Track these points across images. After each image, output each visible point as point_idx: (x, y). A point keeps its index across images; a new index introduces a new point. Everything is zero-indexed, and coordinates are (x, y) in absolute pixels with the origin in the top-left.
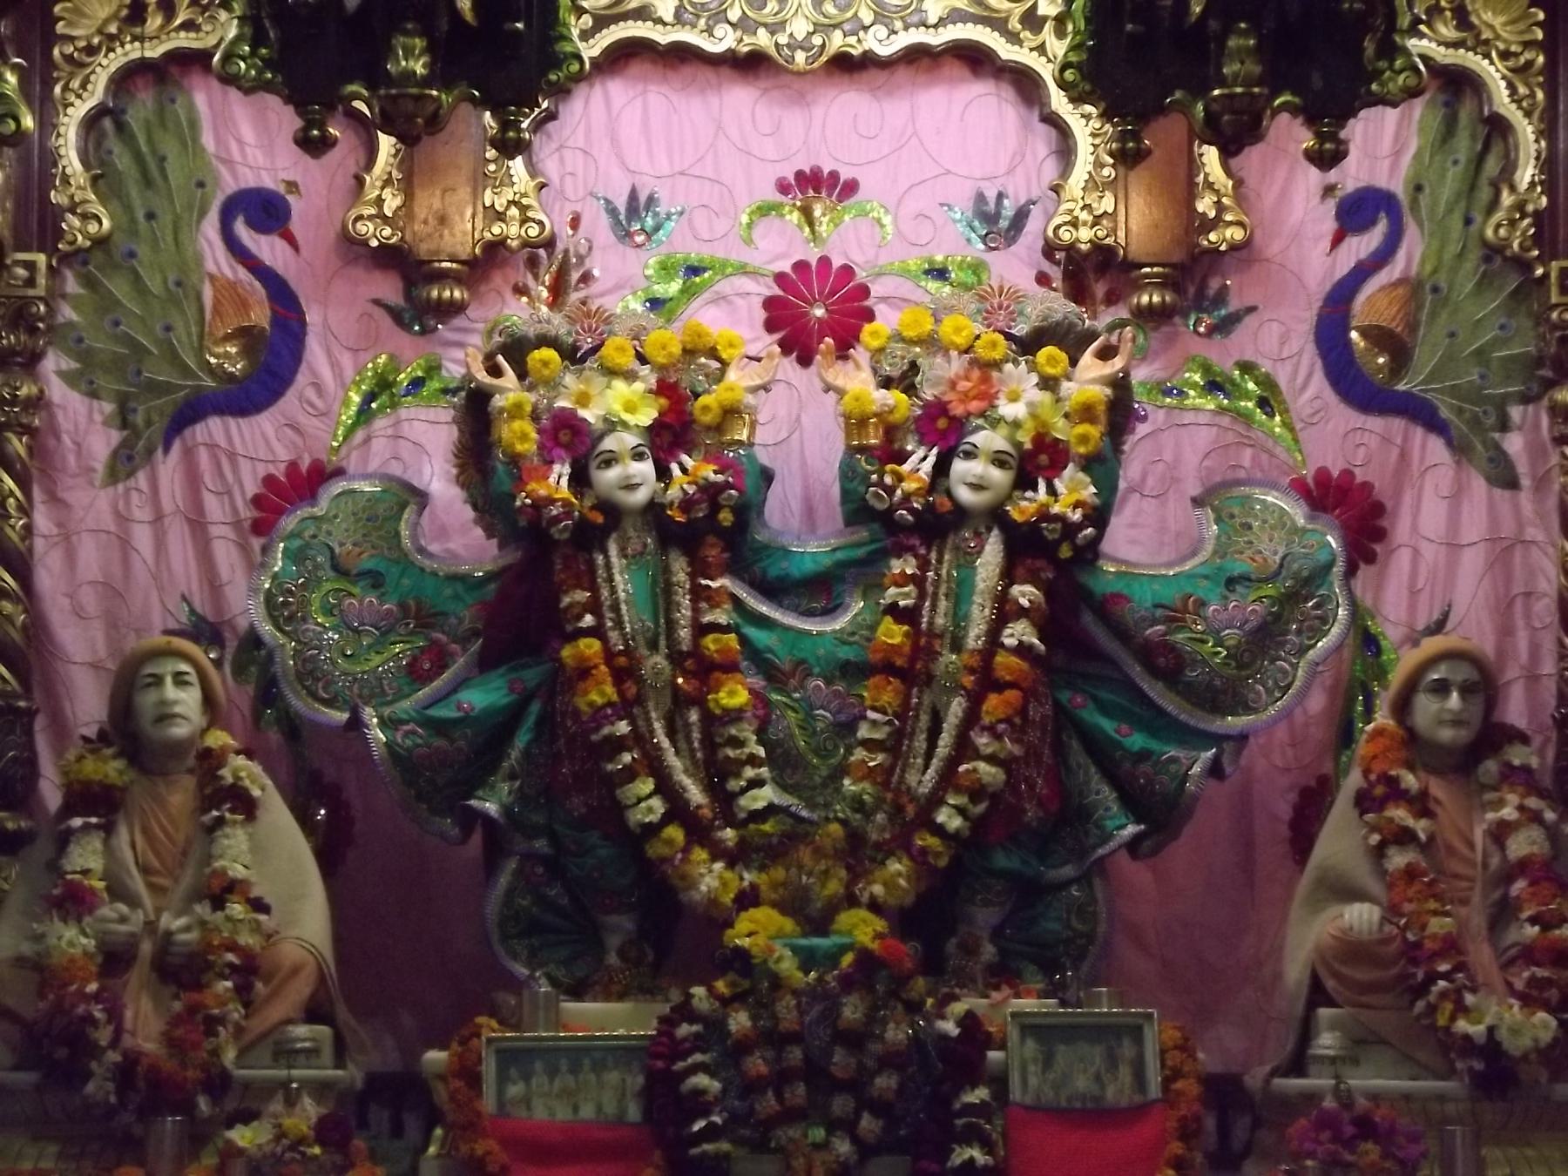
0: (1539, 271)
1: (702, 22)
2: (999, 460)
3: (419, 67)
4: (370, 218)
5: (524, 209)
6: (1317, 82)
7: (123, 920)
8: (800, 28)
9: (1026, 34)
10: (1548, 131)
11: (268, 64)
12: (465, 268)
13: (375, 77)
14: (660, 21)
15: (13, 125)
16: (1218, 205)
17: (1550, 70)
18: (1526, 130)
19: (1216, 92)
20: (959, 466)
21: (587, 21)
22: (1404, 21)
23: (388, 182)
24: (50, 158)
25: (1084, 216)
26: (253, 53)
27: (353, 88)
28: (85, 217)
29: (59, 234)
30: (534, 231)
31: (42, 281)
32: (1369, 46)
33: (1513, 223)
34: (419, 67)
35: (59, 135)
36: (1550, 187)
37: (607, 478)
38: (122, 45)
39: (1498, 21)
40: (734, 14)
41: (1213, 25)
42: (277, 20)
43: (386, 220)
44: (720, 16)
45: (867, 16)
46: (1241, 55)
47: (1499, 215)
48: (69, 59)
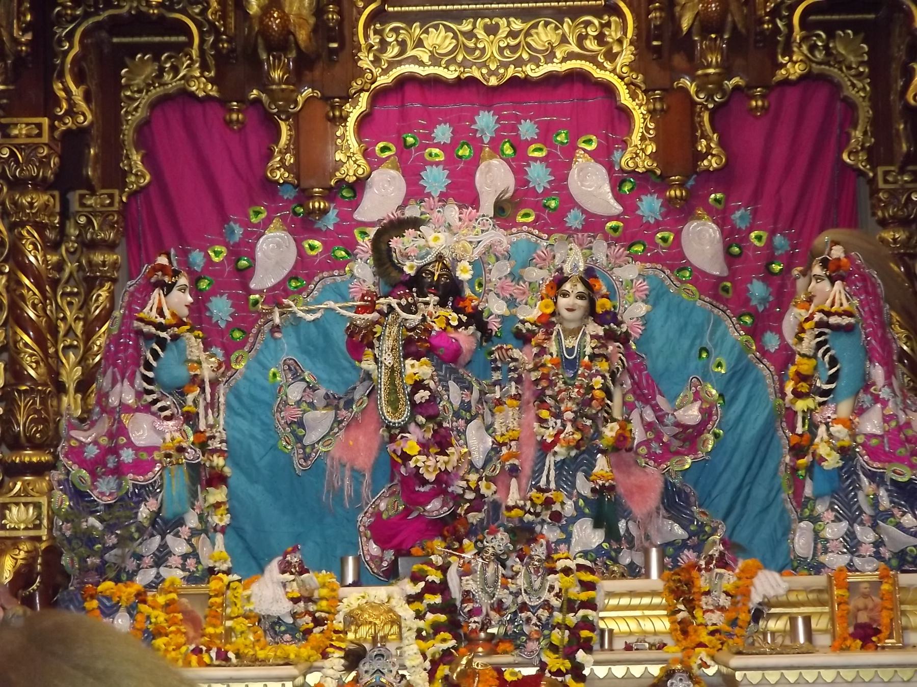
0: (871, 174)
1: (443, 62)
4: (278, 168)
9: (608, 65)
12: (327, 192)
14: (421, 63)
15: (82, 118)
16: (709, 147)
19: (700, 72)
26: (202, 75)
31: (117, 204)
32: (779, 50)
35: (124, 135)
38: (155, 88)
40: (460, 58)
43: (287, 169)
45: (525, 56)
48: (128, 97)
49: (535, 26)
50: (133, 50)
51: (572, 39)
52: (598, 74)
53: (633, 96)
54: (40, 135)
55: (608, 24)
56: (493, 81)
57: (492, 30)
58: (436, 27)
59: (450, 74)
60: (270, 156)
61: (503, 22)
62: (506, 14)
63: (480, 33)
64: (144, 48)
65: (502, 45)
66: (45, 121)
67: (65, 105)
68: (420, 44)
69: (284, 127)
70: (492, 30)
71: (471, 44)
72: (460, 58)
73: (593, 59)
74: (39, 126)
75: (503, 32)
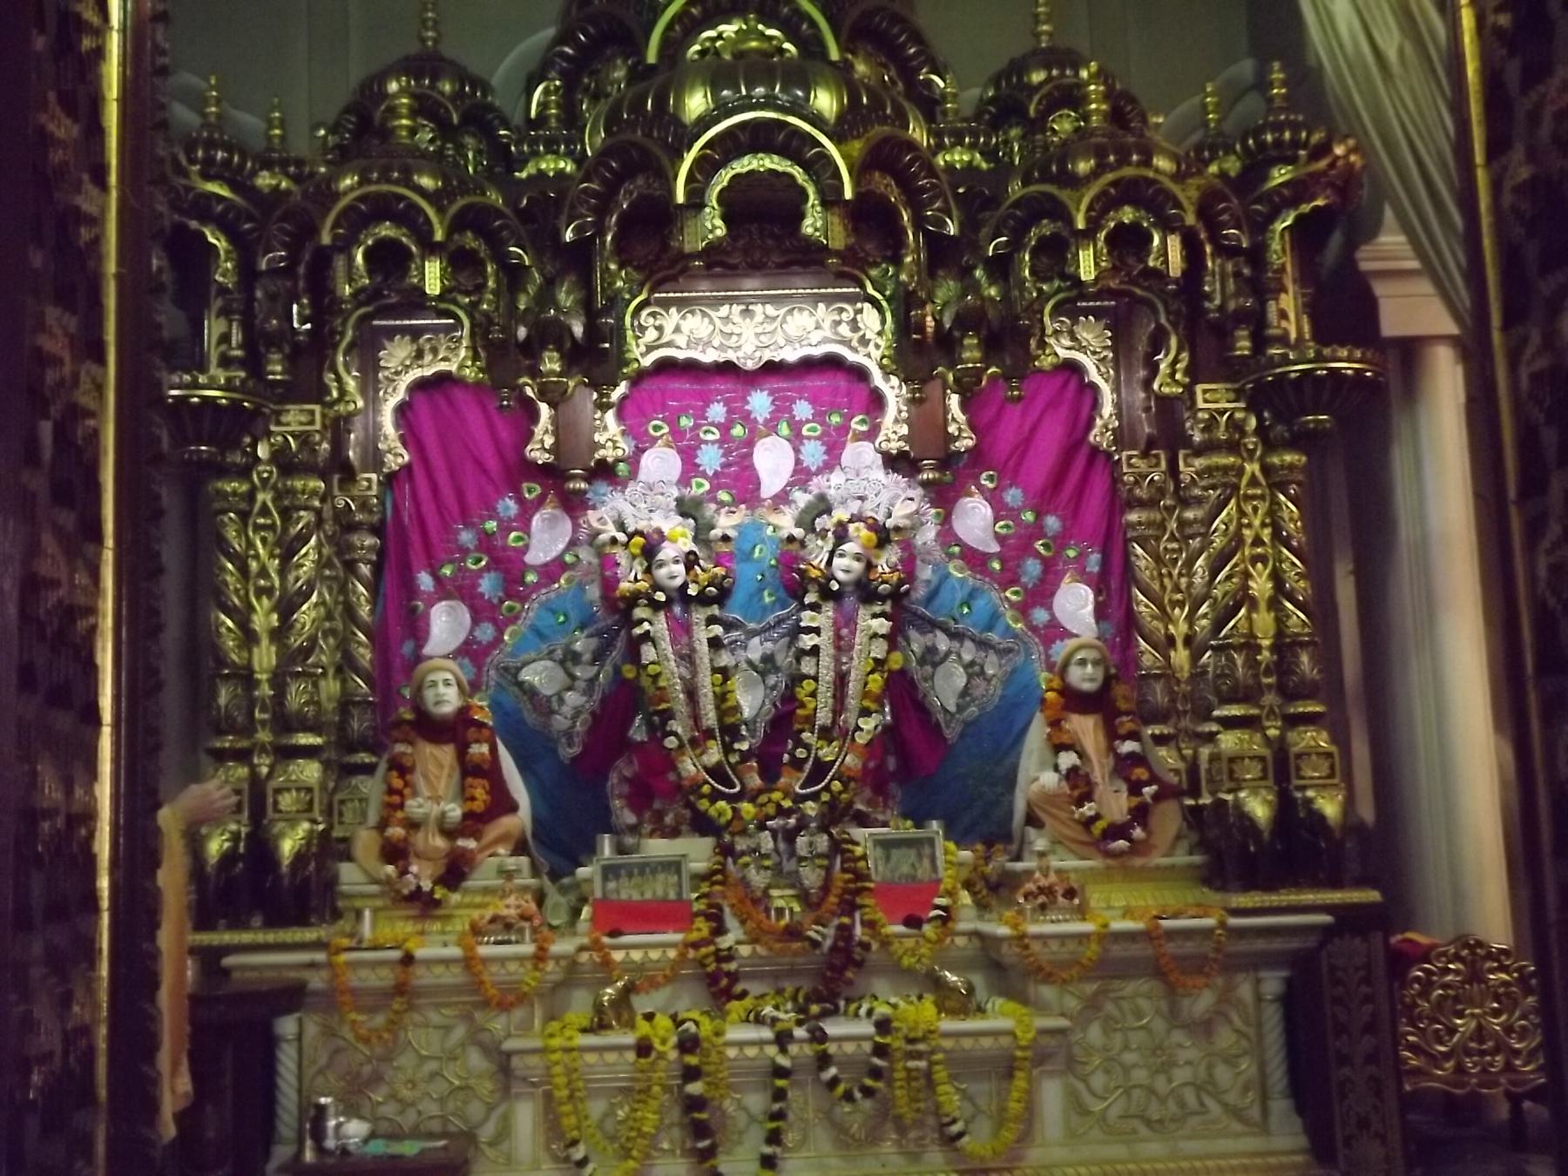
2: (857, 557)
3: (557, 367)
5: (614, 442)
6: (1008, 362)
7: (420, 806)
8: (748, 348)
10: (1116, 389)
11: (481, 370)
13: (535, 373)
16: (960, 429)
17: (1116, 360)
18: (1106, 388)
20: (837, 561)
21: (643, 349)
22: (1049, 331)
23: (546, 431)
24: (378, 427)
25: (893, 436)
27: (522, 380)
28: (396, 455)
29: (383, 463)
30: (620, 453)
32: (1033, 343)
33: (1102, 434)
34: (557, 367)
36: (1119, 416)
37: (661, 573)
39: (1089, 337)
40: (716, 343)
41: (957, 334)
42: (484, 347)
44: (708, 343)
45: (782, 342)
46: (970, 348)
47: (1095, 431)
48: (387, 378)
49: (791, 311)
50: (391, 333)
51: (827, 325)
52: (851, 357)
53: (887, 380)
54: (312, 422)
55: (861, 311)
56: (750, 365)
57: (747, 313)
58: (692, 312)
59: (709, 357)
60: (528, 436)
61: (758, 309)
62: (766, 300)
63: (736, 318)
64: (403, 331)
65: (759, 330)
66: (317, 408)
67: (335, 394)
68: (677, 330)
69: (544, 409)
70: (747, 313)
71: (727, 329)
72: (716, 343)
73: (846, 343)
74: (312, 413)
75: (759, 317)
